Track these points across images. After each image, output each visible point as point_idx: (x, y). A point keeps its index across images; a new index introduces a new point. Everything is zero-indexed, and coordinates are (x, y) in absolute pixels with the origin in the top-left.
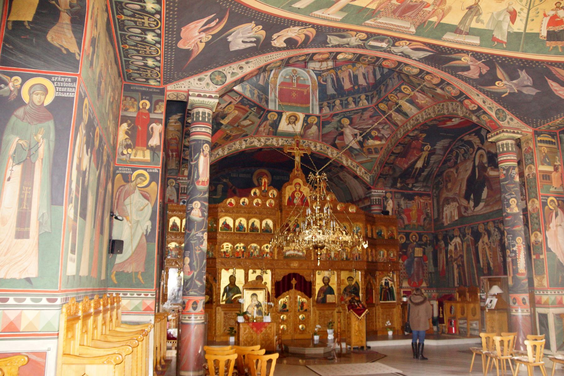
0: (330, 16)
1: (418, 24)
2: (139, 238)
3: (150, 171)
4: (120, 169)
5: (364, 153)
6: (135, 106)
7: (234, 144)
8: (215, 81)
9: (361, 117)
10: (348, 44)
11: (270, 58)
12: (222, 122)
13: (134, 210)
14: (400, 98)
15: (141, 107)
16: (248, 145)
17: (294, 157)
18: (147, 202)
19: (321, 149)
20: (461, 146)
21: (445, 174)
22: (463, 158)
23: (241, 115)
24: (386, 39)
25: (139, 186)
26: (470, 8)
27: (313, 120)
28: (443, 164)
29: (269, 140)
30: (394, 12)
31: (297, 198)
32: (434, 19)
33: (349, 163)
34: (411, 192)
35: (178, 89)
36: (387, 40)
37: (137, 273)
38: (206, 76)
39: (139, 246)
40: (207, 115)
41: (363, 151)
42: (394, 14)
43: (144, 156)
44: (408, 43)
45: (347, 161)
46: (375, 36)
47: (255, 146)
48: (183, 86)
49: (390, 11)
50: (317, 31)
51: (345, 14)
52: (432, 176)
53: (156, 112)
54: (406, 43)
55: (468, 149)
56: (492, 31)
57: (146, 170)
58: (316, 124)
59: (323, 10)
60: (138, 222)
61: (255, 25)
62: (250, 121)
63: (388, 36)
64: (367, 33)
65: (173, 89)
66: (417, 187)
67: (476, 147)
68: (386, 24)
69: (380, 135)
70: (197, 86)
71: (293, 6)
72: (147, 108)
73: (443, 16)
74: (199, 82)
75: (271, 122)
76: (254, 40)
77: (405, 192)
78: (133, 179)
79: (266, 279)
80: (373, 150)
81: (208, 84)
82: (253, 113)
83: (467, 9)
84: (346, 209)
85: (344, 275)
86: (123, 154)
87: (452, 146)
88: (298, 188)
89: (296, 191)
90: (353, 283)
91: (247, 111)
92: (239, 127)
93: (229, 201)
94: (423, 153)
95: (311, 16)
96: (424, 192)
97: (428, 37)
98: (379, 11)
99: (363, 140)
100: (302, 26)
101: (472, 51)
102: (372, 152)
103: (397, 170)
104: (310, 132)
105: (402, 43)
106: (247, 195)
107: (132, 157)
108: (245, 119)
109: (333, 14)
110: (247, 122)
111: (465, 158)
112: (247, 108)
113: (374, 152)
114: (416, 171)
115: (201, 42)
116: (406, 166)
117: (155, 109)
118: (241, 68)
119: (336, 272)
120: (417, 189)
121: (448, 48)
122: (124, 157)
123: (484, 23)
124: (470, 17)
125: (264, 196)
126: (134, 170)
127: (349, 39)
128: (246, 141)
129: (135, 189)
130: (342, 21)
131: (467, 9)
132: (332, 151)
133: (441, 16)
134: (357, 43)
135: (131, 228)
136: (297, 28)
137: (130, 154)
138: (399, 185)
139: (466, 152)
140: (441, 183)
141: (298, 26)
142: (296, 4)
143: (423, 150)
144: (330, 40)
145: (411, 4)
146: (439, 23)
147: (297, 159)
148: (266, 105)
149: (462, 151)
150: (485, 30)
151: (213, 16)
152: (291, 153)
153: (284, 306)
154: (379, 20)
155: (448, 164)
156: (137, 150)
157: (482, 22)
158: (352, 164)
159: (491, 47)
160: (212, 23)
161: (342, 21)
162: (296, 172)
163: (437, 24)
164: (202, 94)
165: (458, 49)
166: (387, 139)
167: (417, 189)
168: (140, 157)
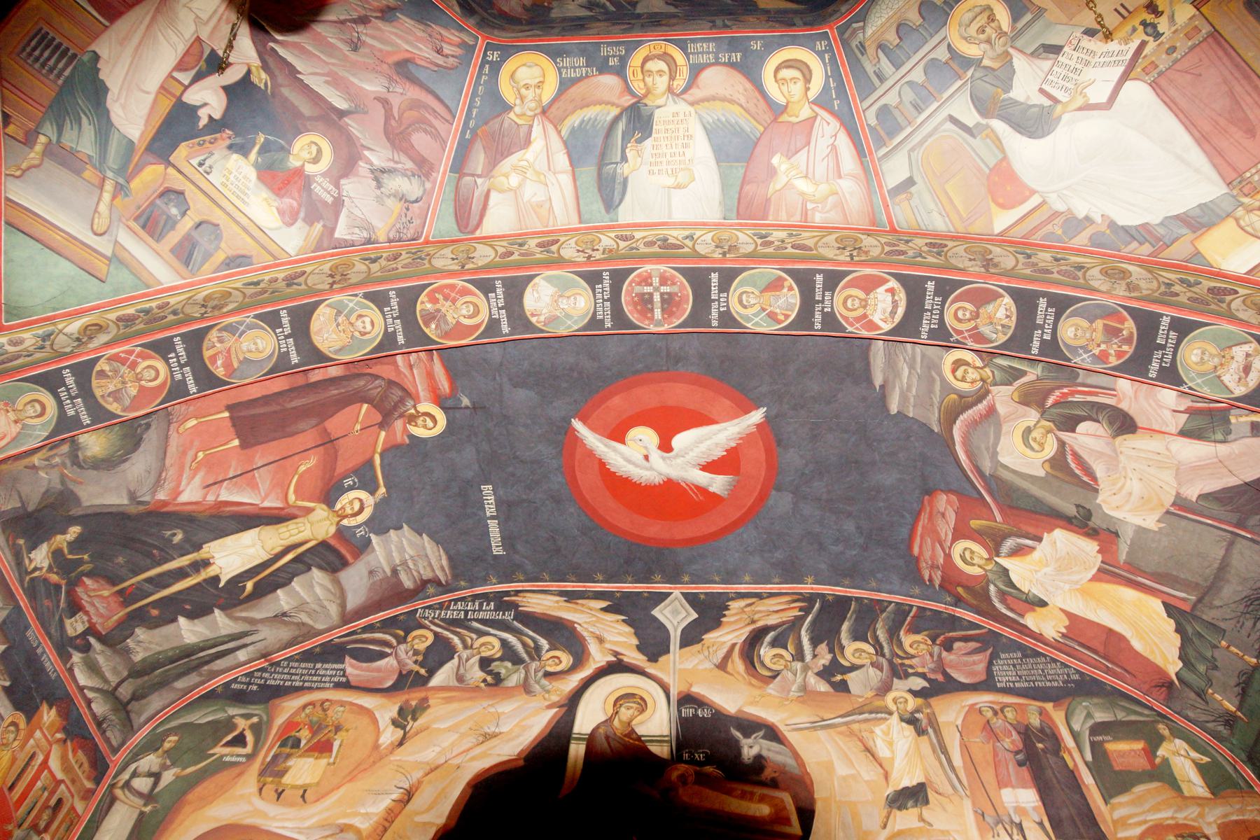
5: (120, 190)
9: (364, 20)
14: (695, 93)
20: (483, 622)
21: (289, 707)
22: (476, 674)
28: (307, 656)
34: (50, 660)
41: (127, 171)
52: (193, 678)
55: (536, 652)
66: (93, 668)
67: (598, 658)
69: (323, 190)
77: (35, 633)
80: (186, 224)
87: (419, 604)
94: (321, 511)
96: (92, 728)
99: (215, 126)
102: (171, 223)
103: (139, 466)
111: (498, 679)
113: (174, 238)
114: (181, 574)
116: (191, 493)
120: (82, 678)
138: (40, 557)
139: (509, 654)
140: (240, 741)
143: (329, 496)
149: (491, 645)
155: (352, 668)
166: (327, 241)
167: (82, 678)
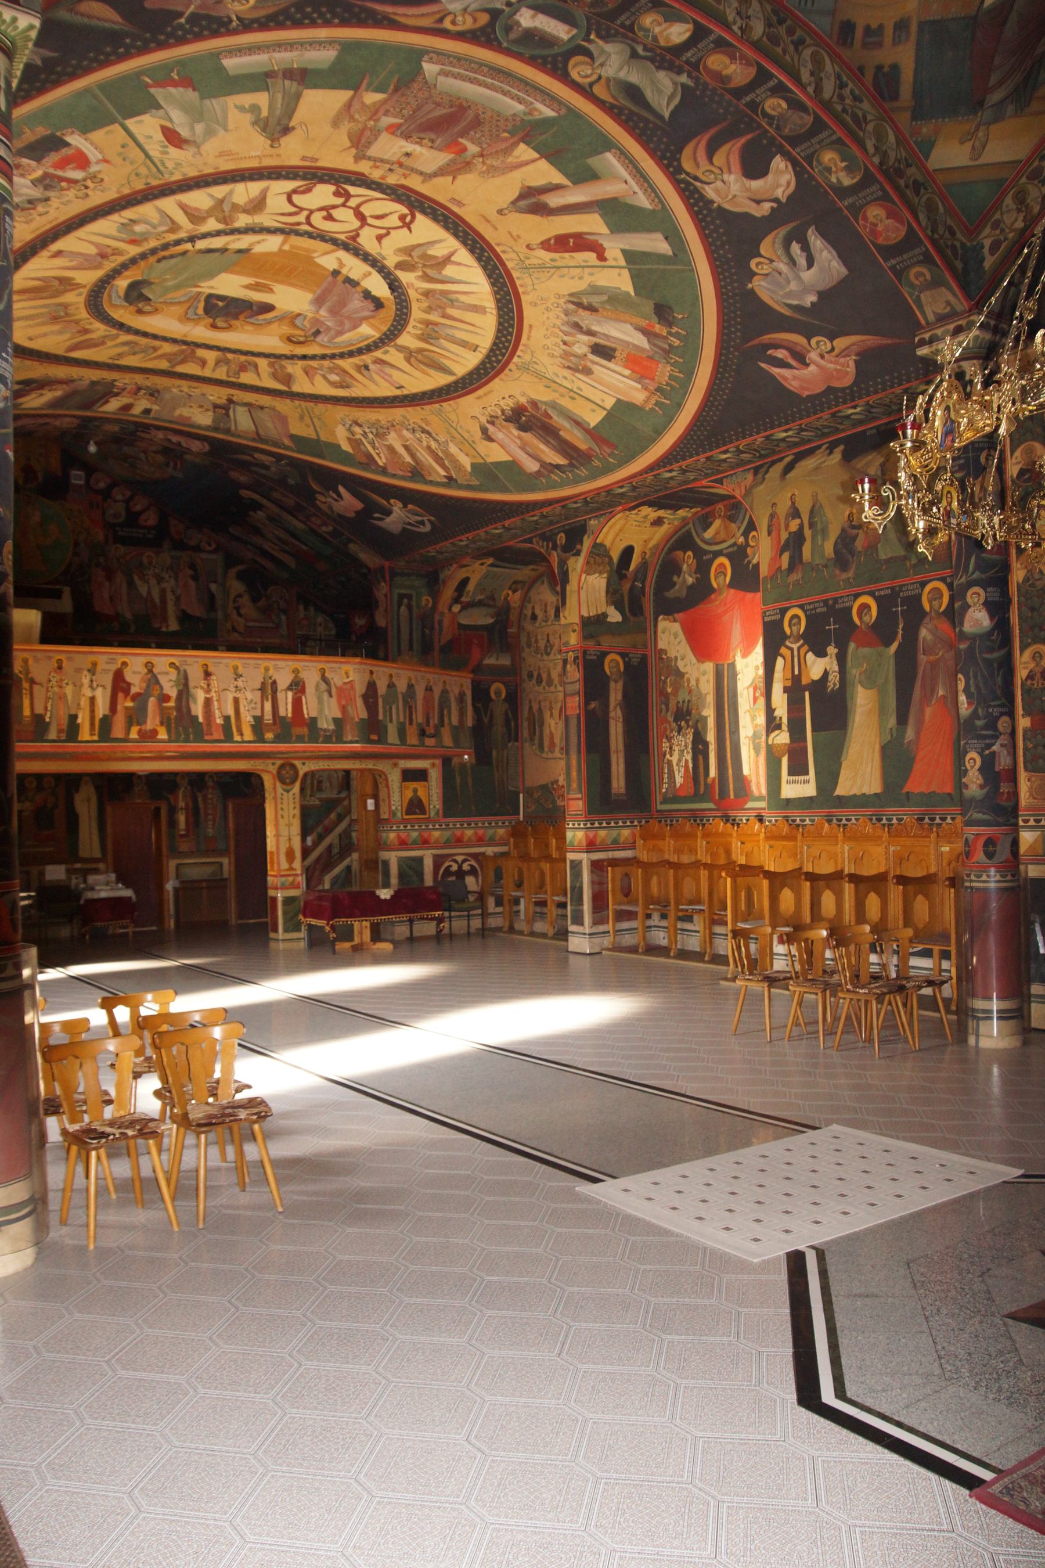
0: (624, 173)
1: (415, 85)
10: (634, 55)
24: (516, 42)
26: (287, 130)
30: (477, 123)
32: (372, 98)
36: (513, 36)
42: (477, 116)
44: (447, 24)
46: (544, 58)
49: (486, 129)
50: (680, 151)
51: (594, 162)
54: (453, 23)
56: (202, 97)
59: (630, 201)
61: (756, 278)
63: (508, 53)
64: (564, 78)
68: (505, 93)
71: (670, 253)
73: (349, 105)
76: (795, 248)
83: (293, 128)
95: (661, 201)
97: (384, 49)
98: (512, 134)
100: (696, 190)
101: (235, 32)
105: (466, 24)
109: (616, 177)
115: (833, 349)
121: (313, 24)
123: (236, 107)
124: (278, 112)
127: (622, 75)
130: (607, 144)
131: (293, 128)
133: (356, 106)
134: (609, 48)
136: (710, 192)
141: (702, 197)
142: (662, 252)
144: (671, 99)
145: (433, 136)
146: (356, 88)
150: (225, 95)
151: (763, 365)
154: (520, 107)
157: (241, 109)
159: (181, 63)
160: (780, 356)
161: (607, 144)
163: (364, 86)
165: (281, 26)
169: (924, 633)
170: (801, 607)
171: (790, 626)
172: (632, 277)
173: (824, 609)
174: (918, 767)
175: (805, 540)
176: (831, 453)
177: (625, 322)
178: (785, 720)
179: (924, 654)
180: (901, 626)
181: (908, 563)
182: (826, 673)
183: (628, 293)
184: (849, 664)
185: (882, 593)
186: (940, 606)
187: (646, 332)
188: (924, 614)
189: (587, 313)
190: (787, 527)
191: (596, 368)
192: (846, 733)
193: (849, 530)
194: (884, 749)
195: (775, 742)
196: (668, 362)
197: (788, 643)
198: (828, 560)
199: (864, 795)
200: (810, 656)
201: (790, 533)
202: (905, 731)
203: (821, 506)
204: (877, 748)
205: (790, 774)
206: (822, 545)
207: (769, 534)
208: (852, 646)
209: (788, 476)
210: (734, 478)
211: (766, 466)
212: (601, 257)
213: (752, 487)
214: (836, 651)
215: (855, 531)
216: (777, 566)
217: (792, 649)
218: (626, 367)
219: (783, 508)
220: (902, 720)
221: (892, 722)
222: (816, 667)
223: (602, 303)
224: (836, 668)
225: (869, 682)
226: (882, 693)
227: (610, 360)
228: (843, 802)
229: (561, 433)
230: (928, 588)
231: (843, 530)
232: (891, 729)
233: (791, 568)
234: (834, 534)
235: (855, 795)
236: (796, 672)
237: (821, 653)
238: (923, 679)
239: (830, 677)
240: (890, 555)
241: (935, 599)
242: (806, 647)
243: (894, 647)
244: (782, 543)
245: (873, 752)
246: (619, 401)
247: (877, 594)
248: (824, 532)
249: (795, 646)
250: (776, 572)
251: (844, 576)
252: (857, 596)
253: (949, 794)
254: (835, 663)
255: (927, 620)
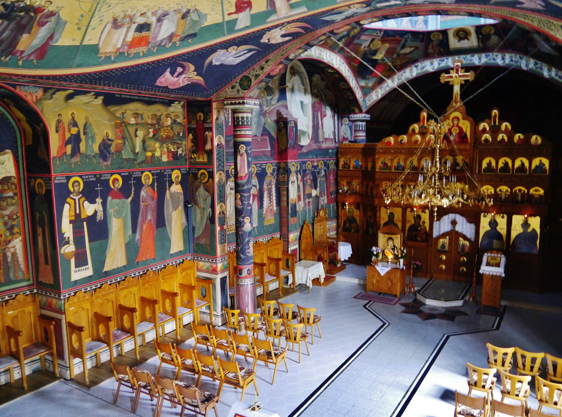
2: (205, 221)
3: (208, 170)
4: (191, 169)
6: (195, 119)
7: (405, 73)
8: (243, 87)
11: (286, 50)
12: (375, 58)
13: (201, 200)
15: (198, 119)
16: (419, 71)
17: (452, 86)
18: (208, 194)
19: (512, 60)
23: (395, 46)
25: (203, 182)
27: (488, 29)
29: (443, 61)
31: (454, 134)
33: (553, 73)
35: (218, 99)
37: (206, 245)
38: (236, 83)
39: (206, 226)
40: (240, 119)
43: (204, 159)
45: (549, 70)
47: (427, 70)
48: (222, 96)
53: (208, 122)
57: (205, 169)
58: (495, 34)
60: (204, 208)
62: (410, 47)
65: (216, 100)
70: (231, 94)
72: (202, 119)
74: (232, 90)
75: (437, 42)
78: (199, 177)
79: (424, 218)
81: (238, 91)
82: (409, 40)
84: (527, 139)
85: (518, 220)
86: (192, 158)
88: (456, 122)
89: (453, 126)
90: (530, 230)
91: (400, 41)
92: (401, 56)
93: (387, 140)
104: (491, 44)
106: (405, 133)
107: (197, 160)
108: (403, 47)
110: (407, 50)
112: (398, 37)
117: (207, 120)
118: (262, 68)
119: (506, 216)
122: (192, 160)
125: (423, 133)
126: (199, 170)
128: (417, 67)
129: (201, 184)
132: (527, 61)
135: (200, 212)
137: (196, 158)
147: (457, 89)
148: (424, 27)
152: (449, 82)
153: (443, 246)
156: (199, 155)
158: (557, 75)
162: (454, 104)
164: (233, 102)
168: (201, 160)
169: (143, 193)
170: (81, 177)
171: (73, 186)
172: (217, 25)
173: (94, 179)
174: (141, 250)
175: (81, 140)
176: (96, 98)
177: (177, 28)
178: (71, 239)
179: (143, 202)
180: (133, 190)
181: (136, 162)
182: (96, 212)
183: (204, 24)
184: (108, 207)
185: (124, 174)
186: (149, 183)
187: (171, 37)
188: (143, 185)
189: (181, 16)
190: (69, 131)
191: (124, 29)
192: (108, 241)
193: (107, 141)
194: (126, 245)
195: (66, 252)
196: (149, 49)
197: (71, 196)
198: (96, 154)
199: (118, 268)
200: (86, 203)
201: (71, 134)
202: (135, 236)
203: (91, 124)
204: (124, 245)
205: (76, 267)
206: (92, 146)
207: (57, 131)
208: (110, 198)
209: (69, 101)
210: (22, 87)
211: (53, 91)
212: (229, 14)
213: (41, 99)
214: (101, 200)
215: (110, 142)
216: (64, 152)
217: (75, 200)
218: (134, 39)
219: (66, 119)
220: (134, 231)
221: (130, 232)
222: (89, 209)
223: (191, 19)
224: (102, 209)
225: (118, 214)
226: (125, 220)
227: (135, 31)
228: (107, 274)
229: (25, 36)
230: (145, 174)
231: (104, 140)
232: (129, 236)
233: (73, 154)
234: (99, 141)
235: (114, 269)
236: (78, 212)
237: (93, 202)
238: (142, 213)
239: (98, 214)
240: (128, 157)
241: (147, 179)
242: (84, 199)
243: (130, 199)
244: (67, 139)
245: (122, 247)
246: (97, 45)
247: (122, 174)
248: (93, 138)
249: (77, 198)
250: (62, 155)
251: (105, 163)
252: (112, 174)
253: (154, 259)
254: (101, 206)
255: (144, 188)
